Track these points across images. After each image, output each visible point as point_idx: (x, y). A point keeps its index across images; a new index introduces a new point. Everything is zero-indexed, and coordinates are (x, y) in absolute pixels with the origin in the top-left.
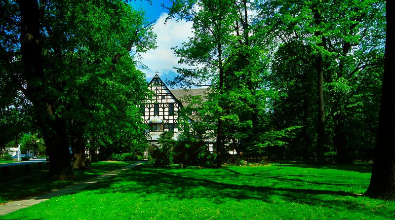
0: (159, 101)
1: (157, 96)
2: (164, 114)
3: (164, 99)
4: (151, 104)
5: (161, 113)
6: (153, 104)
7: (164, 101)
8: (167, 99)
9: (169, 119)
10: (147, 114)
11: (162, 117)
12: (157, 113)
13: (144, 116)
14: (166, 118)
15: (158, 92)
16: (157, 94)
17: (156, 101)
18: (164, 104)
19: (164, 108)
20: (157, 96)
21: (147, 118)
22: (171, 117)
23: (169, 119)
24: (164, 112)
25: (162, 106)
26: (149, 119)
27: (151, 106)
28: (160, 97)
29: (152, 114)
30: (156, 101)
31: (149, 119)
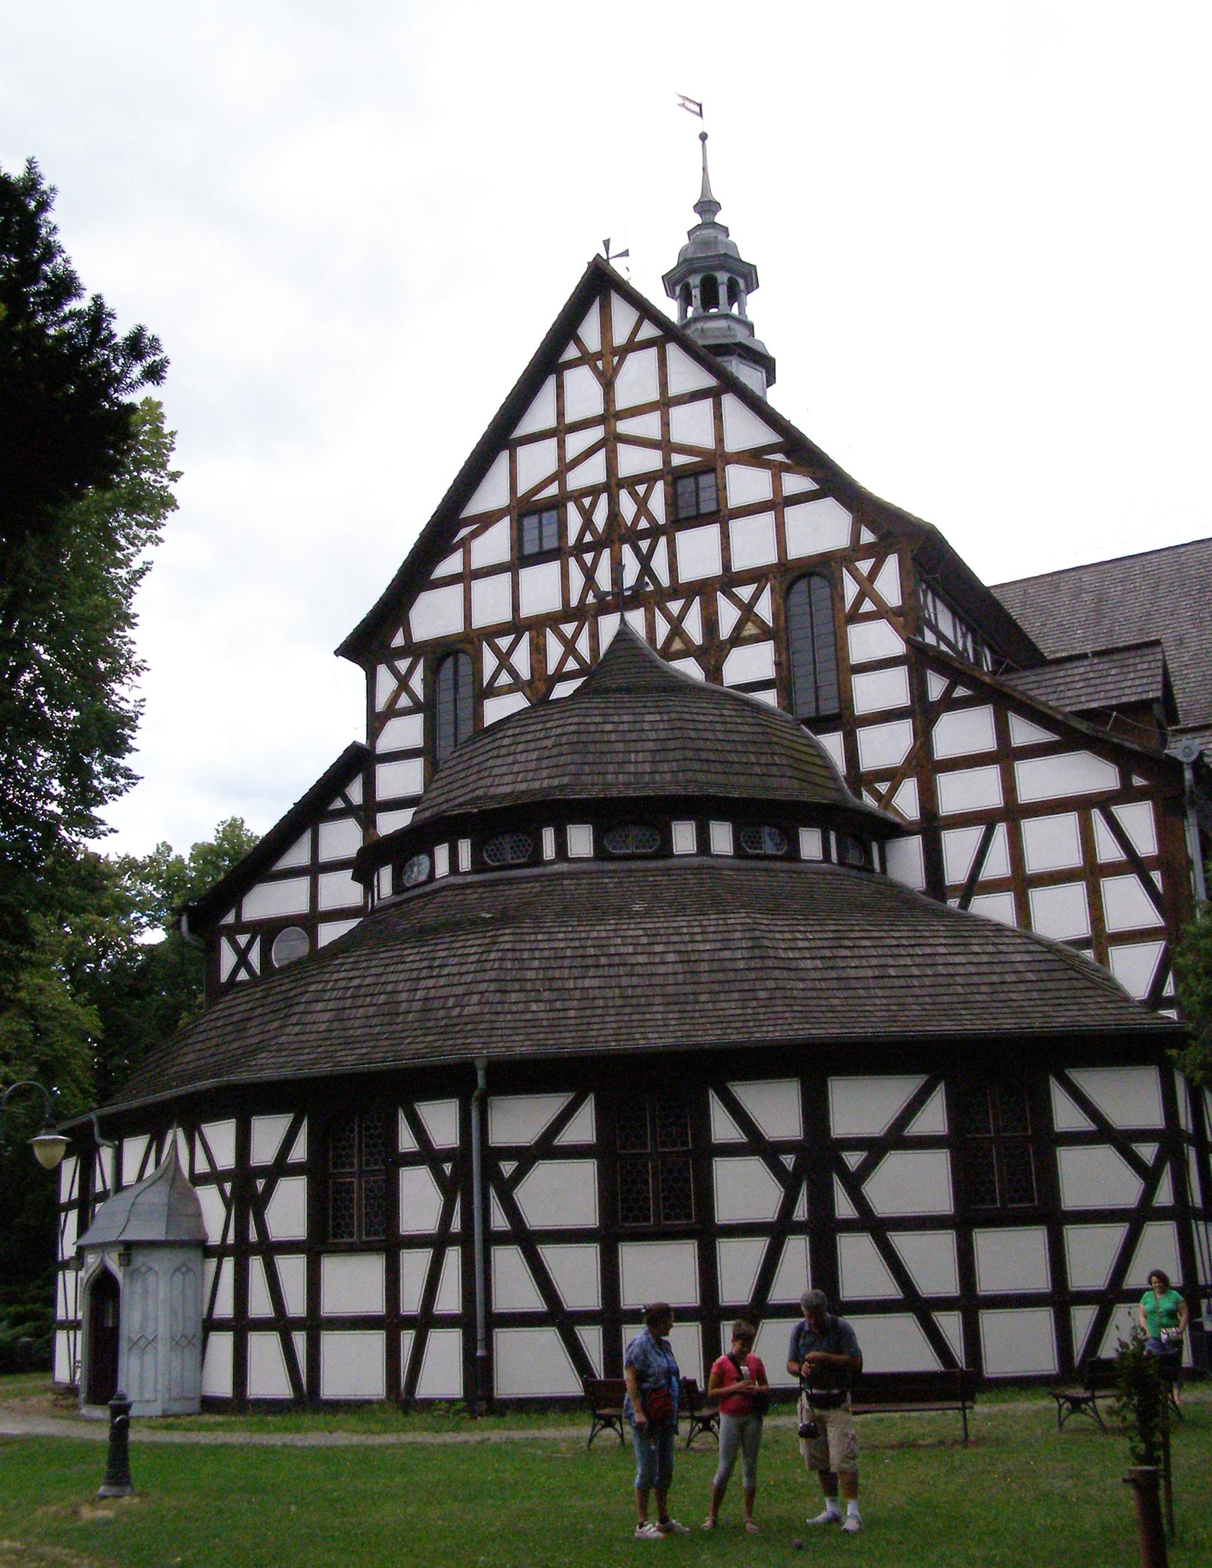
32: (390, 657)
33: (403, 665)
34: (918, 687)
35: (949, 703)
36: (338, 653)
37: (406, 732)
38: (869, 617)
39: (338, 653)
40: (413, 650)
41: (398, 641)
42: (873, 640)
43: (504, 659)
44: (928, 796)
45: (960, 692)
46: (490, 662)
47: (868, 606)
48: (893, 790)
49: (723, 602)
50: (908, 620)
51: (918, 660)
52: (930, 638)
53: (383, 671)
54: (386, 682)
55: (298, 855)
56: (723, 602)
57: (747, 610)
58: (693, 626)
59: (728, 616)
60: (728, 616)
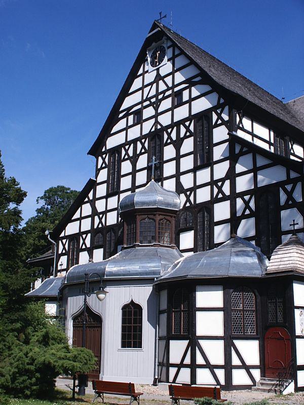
5: (169, 169)
7: (181, 113)
8: (191, 100)
12: (156, 173)
14: (187, 181)
17: (157, 122)
22: (204, 176)
30: (157, 122)
32: (101, 154)
33: (104, 156)
34: (231, 148)
35: (242, 154)
36: (88, 154)
37: (103, 175)
38: (220, 125)
39: (88, 154)
40: (105, 153)
41: (104, 150)
42: (220, 134)
44: (233, 186)
45: (245, 149)
46: (123, 152)
47: (220, 122)
48: (222, 185)
50: (232, 126)
51: (233, 140)
52: (240, 134)
53: (100, 158)
54: (100, 161)
57: (187, 128)
58: (174, 136)
59: (183, 130)
60: (183, 130)
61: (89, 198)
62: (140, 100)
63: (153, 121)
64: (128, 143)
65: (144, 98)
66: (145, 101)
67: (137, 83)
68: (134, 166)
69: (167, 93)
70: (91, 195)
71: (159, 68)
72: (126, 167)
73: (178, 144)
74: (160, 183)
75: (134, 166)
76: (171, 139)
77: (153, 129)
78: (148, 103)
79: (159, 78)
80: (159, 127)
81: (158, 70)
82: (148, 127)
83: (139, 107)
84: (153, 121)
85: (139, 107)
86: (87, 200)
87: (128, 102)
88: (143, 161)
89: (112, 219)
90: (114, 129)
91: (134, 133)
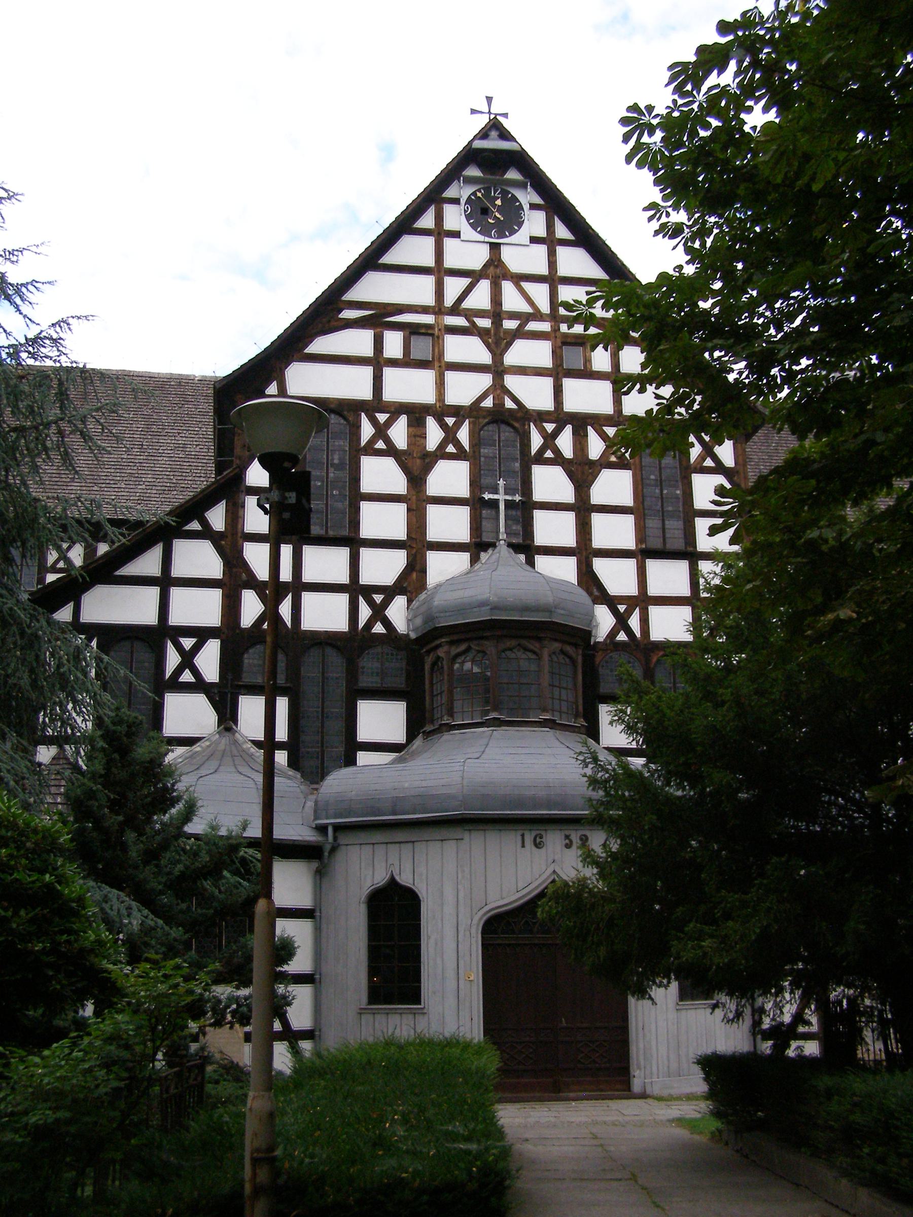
0: (535, 394)
1: (498, 342)
2: (584, 529)
3: (587, 373)
4: (441, 411)
5: (555, 529)
6: (458, 412)
9: (643, 600)
10: (382, 521)
11: (564, 570)
13: (353, 542)
14: (618, 577)
15: (512, 300)
16: (497, 313)
18: (581, 423)
19: (582, 472)
20: (498, 342)
21: (382, 568)
23: (643, 600)
24: (583, 509)
25: (565, 442)
26: (412, 580)
27: (434, 435)
28: (538, 353)
29: (449, 524)
30: (499, 389)
31: (412, 580)
43: (381, 431)
46: (367, 430)
49: (591, 433)
55: (149, 563)
56: (591, 433)
61: (205, 523)
62: (429, 300)
63: (486, 380)
64: (375, 405)
65: (449, 301)
66: (455, 310)
67: (415, 250)
68: (417, 480)
69: (533, 326)
70: (217, 518)
71: (499, 244)
72: (380, 474)
73: (582, 472)
74: (522, 557)
75: (417, 480)
76: (557, 451)
77: (488, 403)
78: (460, 321)
79: (495, 271)
80: (509, 404)
81: (495, 248)
82: (464, 389)
83: (429, 319)
84: (486, 380)
85: (429, 319)
86: (195, 526)
87: (375, 288)
88: (450, 477)
89: (325, 614)
90: (321, 345)
91: (409, 386)
